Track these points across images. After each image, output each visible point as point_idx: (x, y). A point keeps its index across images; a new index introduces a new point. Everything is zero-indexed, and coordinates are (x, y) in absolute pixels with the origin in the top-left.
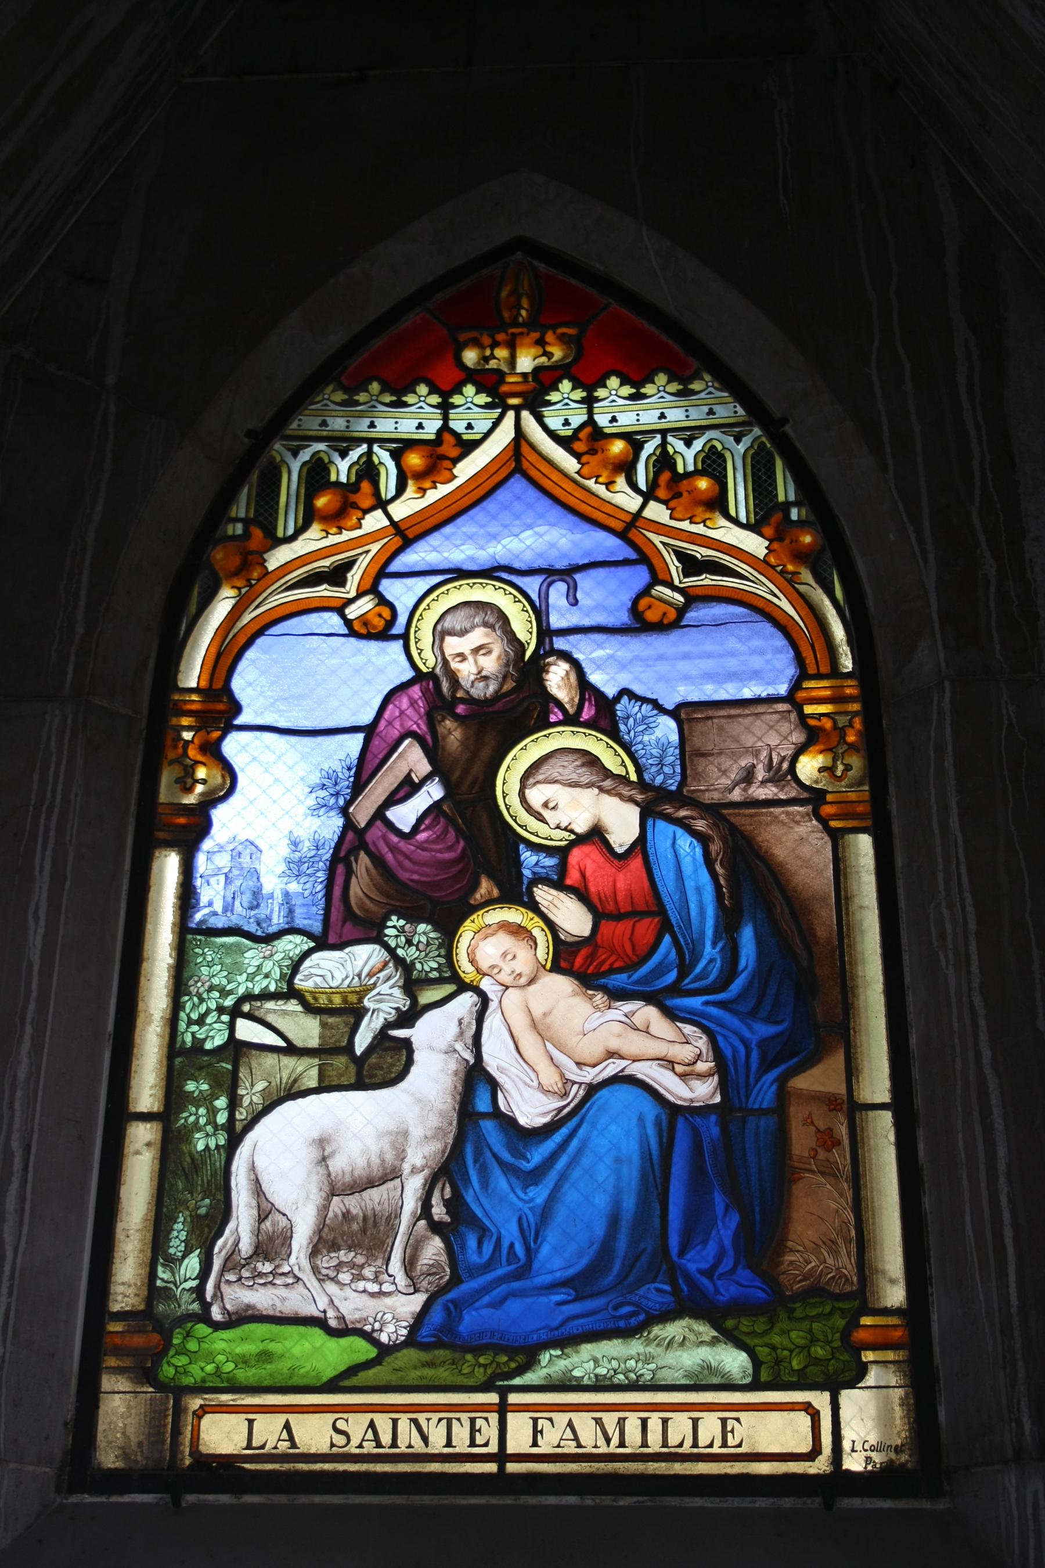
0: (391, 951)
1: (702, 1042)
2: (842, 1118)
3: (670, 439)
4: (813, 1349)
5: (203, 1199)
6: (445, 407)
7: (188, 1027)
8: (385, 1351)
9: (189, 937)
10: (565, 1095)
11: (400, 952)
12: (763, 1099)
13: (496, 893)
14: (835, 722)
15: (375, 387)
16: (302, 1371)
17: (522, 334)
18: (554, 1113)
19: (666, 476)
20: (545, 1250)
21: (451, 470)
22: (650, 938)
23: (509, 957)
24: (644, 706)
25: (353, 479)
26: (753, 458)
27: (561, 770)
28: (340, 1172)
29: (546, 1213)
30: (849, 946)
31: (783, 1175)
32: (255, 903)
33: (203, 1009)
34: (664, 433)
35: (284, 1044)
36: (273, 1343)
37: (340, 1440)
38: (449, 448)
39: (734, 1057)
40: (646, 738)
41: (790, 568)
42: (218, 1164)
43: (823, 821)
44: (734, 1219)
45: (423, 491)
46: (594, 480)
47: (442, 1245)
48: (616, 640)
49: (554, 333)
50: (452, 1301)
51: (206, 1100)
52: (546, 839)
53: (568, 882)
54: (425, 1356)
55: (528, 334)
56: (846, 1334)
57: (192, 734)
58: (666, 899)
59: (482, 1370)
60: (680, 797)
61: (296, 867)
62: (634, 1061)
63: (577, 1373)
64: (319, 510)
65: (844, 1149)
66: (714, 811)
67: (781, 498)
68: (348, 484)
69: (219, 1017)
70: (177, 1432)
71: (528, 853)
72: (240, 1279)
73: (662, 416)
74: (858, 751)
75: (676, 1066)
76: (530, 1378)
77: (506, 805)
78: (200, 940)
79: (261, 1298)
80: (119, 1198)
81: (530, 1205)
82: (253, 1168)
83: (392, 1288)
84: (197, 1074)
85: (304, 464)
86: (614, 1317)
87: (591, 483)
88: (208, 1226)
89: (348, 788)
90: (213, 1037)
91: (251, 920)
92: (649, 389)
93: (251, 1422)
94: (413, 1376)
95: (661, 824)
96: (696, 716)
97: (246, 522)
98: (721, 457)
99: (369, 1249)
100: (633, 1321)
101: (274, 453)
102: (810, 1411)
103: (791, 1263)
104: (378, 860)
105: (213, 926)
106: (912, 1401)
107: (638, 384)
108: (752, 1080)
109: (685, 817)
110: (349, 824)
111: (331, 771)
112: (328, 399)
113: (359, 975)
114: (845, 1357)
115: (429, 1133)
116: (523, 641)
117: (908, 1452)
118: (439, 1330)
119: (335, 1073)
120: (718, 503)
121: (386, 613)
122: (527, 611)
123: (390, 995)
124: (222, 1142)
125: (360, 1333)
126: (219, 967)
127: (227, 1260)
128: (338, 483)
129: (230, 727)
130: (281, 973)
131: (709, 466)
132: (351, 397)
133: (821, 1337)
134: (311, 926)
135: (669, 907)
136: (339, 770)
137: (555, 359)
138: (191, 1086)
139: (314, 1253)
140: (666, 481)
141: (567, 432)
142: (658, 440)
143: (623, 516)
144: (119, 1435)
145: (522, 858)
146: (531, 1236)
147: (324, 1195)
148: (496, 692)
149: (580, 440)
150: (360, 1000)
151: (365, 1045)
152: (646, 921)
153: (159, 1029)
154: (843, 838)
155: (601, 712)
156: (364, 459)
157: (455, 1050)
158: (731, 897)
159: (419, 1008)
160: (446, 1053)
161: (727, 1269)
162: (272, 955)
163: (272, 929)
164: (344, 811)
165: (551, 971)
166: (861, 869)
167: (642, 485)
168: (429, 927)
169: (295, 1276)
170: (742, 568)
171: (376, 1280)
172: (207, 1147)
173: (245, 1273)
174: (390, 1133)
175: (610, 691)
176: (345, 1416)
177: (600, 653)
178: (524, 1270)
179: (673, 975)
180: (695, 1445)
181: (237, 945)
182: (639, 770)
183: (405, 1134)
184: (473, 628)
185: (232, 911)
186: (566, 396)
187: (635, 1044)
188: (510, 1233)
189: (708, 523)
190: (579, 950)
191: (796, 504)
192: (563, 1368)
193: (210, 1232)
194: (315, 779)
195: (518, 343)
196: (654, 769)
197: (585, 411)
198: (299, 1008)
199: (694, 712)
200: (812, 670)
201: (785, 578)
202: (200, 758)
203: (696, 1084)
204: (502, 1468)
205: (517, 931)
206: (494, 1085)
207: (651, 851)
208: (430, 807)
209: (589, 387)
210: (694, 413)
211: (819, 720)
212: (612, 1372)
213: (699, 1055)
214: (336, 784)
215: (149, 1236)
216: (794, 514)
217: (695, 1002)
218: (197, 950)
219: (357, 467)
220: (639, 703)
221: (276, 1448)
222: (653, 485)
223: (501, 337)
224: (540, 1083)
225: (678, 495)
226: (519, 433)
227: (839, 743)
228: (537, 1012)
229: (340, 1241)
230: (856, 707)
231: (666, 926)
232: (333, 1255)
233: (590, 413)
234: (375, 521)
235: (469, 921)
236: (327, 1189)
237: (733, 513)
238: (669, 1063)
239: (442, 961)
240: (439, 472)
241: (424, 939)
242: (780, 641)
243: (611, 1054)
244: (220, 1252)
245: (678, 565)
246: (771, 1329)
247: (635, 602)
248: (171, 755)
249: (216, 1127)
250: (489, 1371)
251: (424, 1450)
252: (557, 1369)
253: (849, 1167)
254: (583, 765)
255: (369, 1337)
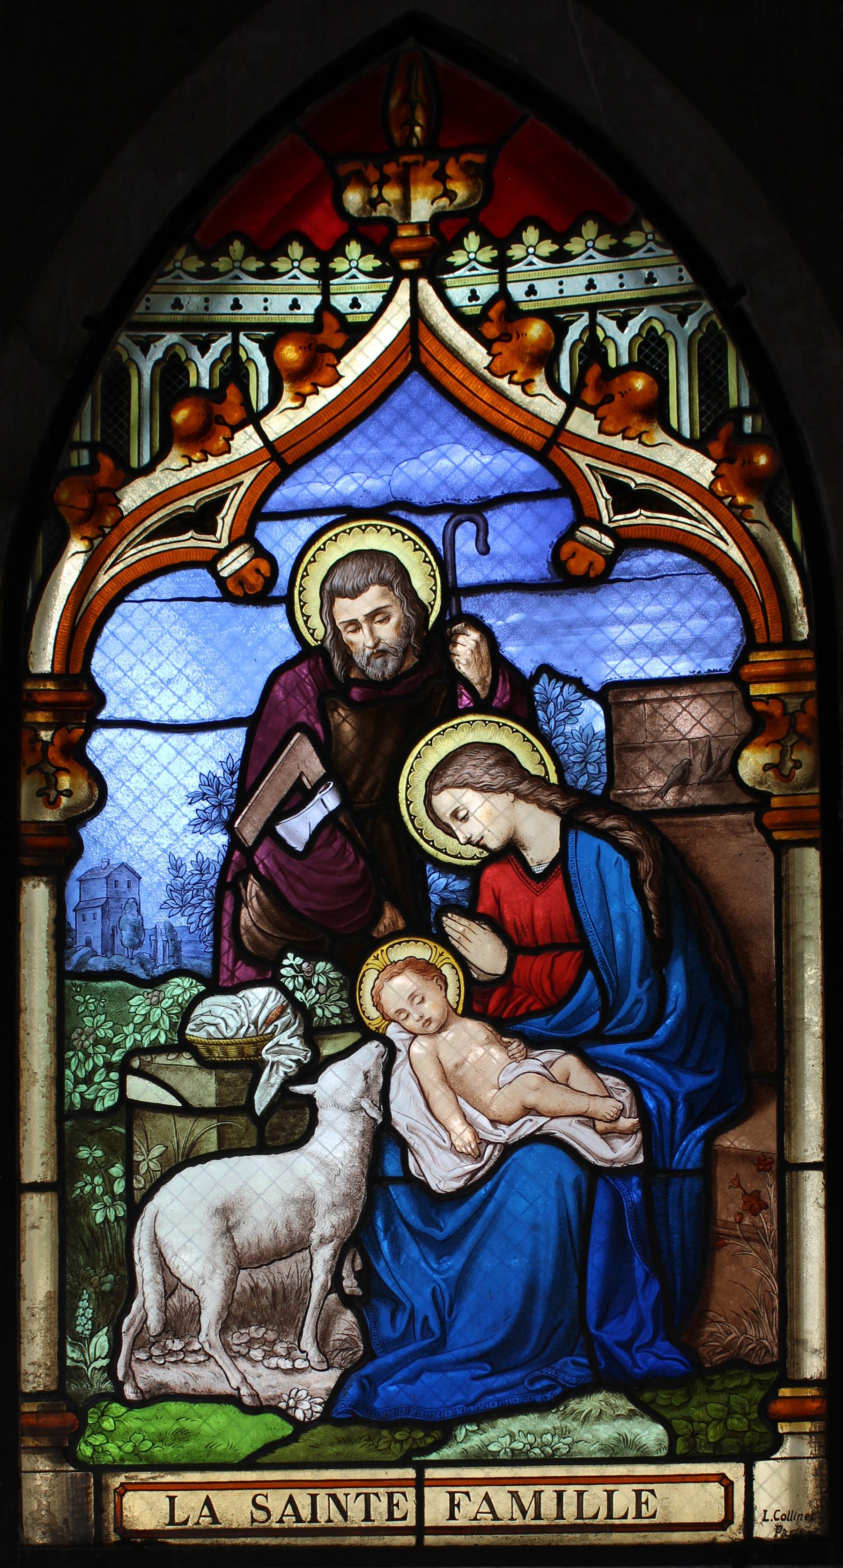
0: (289, 995)
1: (625, 1096)
2: (771, 1178)
3: (600, 318)
4: (729, 1421)
5: (107, 1275)
6: (325, 275)
7: (75, 1087)
8: (301, 1427)
9: (68, 982)
10: (480, 1156)
11: (299, 995)
12: (688, 1159)
13: (401, 924)
14: (784, 706)
15: (237, 248)
16: (219, 1449)
17: (416, 163)
18: (467, 1177)
19: (594, 371)
20: (459, 1324)
21: (334, 367)
22: (571, 974)
23: (417, 1000)
24: (566, 687)
25: (217, 383)
26: (700, 345)
27: (471, 770)
28: (246, 1244)
29: (460, 1284)
30: (788, 983)
31: (706, 1239)
32: (137, 941)
33: (89, 1065)
34: (593, 309)
35: (178, 1104)
36: (188, 1422)
37: (260, 1515)
38: (332, 337)
39: (659, 1112)
40: (568, 729)
41: (741, 500)
42: (119, 1237)
43: (766, 832)
44: (655, 1287)
45: (301, 398)
46: (506, 379)
47: (354, 1319)
48: (531, 600)
49: (457, 161)
50: (366, 1377)
51: (101, 1167)
52: (456, 857)
53: (481, 909)
54: (340, 1433)
55: (424, 164)
56: (763, 1406)
57: (50, 733)
58: (589, 929)
59: (398, 1445)
60: (606, 804)
61: (179, 896)
62: (552, 1118)
63: (493, 1448)
64: (179, 427)
65: (771, 1214)
66: (645, 820)
67: (733, 402)
68: (211, 391)
69: (107, 1075)
70: (100, 1509)
71: (436, 875)
72: (150, 1357)
73: (591, 285)
74: (809, 743)
75: (597, 1122)
76: (447, 1453)
77: (410, 815)
78: (80, 986)
79: (174, 1376)
80: (20, 1276)
81: (444, 1277)
82: (155, 1240)
83: (305, 1364)
84: (89, 1138)
85: (157, 363)
86: (531, 1391)
87: (503, 383)
88: (113, 1302)
89: (231, 797)
90: (103, 1098)
91: (134, 961)
92: (575, 246)
93: (172, 1499)
94: (330, 1452)
95: (584, 837)
96: (625, 699)
97: (93, 447)
98: (662, 343)
99: (280, 1324)
100: (549, 1396)
101: (119, 348)
102: (725, 1482)
103: (711, 1334)
104: (266, 884)
105: (93, 969)
106: (825, 1472)
107: (561, 238)
108: (677, 1137)
109: (612, 828)
110: (235, 842)
111: (211, 776)
112: (181, 268)
113: (255, 1023)
114: (762, 1429)
115: (337, 1200)
116: (426, 603)
117: (818, 1520)
118: (354, 1407)
119: (234, 1135)
120: (655, 411)
121: (264, 567)
122: (430, 563)
123: (290, 1045)
124: (121, 1213)
125: (275, 1410)
126: (103, 1017)
127: (135, 1338)
128: (199, 389)
129: (95, 725)
130: (170, 1021)
131: (647, 357)
132: (208, 264)
133: (739, 1410)
134: (200, 966)
135: (592, 938)
136: (220, 773)
137: (458, 201)
138: (84, 1153)
139: (224, 1330)
140: (596, 382)
141: (473, 310)
142: (584, 321)
143: (542, 429)
144: (43, 1513)
145: (429, 880)
146: (447, 1305)
147: (230, 1268)
148: (396, 671)
149: (491, 321)
150: (258, 1052)
151: (265, 1104)
152: (568, 955)
153: (44, 1090)
154: (787, 852)
155: (514, 694)
156: (229, 354)
157: (362, 1108)
158: (660, 926)
159: (321, 1060)
160: (352, 1111)
161: (646, 1340)
162: (160, 1002)
163: (159, 971)
164: (228, 827)
165: (464, 1015)
166: (805, 891)
167: (566, 386)
168: (329, 966)
169: (206, 1354)
170: (681, 498)
171: (288, 1356)
172: (106, 1218)
173: (156, 1352)
174: (295, 1201)
175: (527, 667)
176: (264, 1492)
177: (514, 618)
178: (440, 1345)
179: (594, 1020)
180: (610, 1516)
181: (121, 990)
182: (560, 770)
183: (312, 1201)
184: (367, 587)
185: (112, 951)
186: (472, 256)
187: (553, 1098)
188: (423, 1305)
189: (644, 438)
190: (494, 991)
191: (751, 410)
192: (479, 1443)
193: (116, 1309)
194: (193, 784)
195: (412, 177)
196: (577, 768)
197: (495, 278)
198: (192, 1063)
199: (624, 694)
200: (760, 639)
201: (733, 513)
202: (62, 763)
203: (618, 1142)
204: (420, 1540)
205: (425, 969)
206: (404, 1147)
207: (572, 870)
208: (325, 818)
209: (501, 239)
210: (630, 281)
211: (767, 703)
212: (528, 1447)
213: (622, 1111)
214: (218, 792)
215: (55, 1314)
216: (748, 424)
217: (619, 1050)
218: (77, 998)
219: (221, 365)
220: (560, 684)
221: (198, 1523)
222: (579, 384)
223: (391, 169)
224: (452, 1144)
225: (608, 399)
226: (417, 312)
227: (788, 733)
228: (449, 1063)
229: (250, 1317)
230: (810, 686)
231: (588, 962)
232: (243, 1331)
233: (503, 282)
234: (246, 442)
235: (372, 957)
236: (232, 1261)
237: (674, 424)
238: (588, 1119)
239: (345, 1005)
240: (319, 370)
241: (323, 980)
242: (725, 599)
243: (529, 1111)
244: (128, 1330)
245: (608, 497)
246: (688, 1401)
247: (557, 548)
248: (30, 760)
249: (113, 1196)
250: (406, 1447)
251: (343, 1524)
252: (473, 1443)
253: (775, 1233)
254: (495, 765)
255: (285, 1415)
